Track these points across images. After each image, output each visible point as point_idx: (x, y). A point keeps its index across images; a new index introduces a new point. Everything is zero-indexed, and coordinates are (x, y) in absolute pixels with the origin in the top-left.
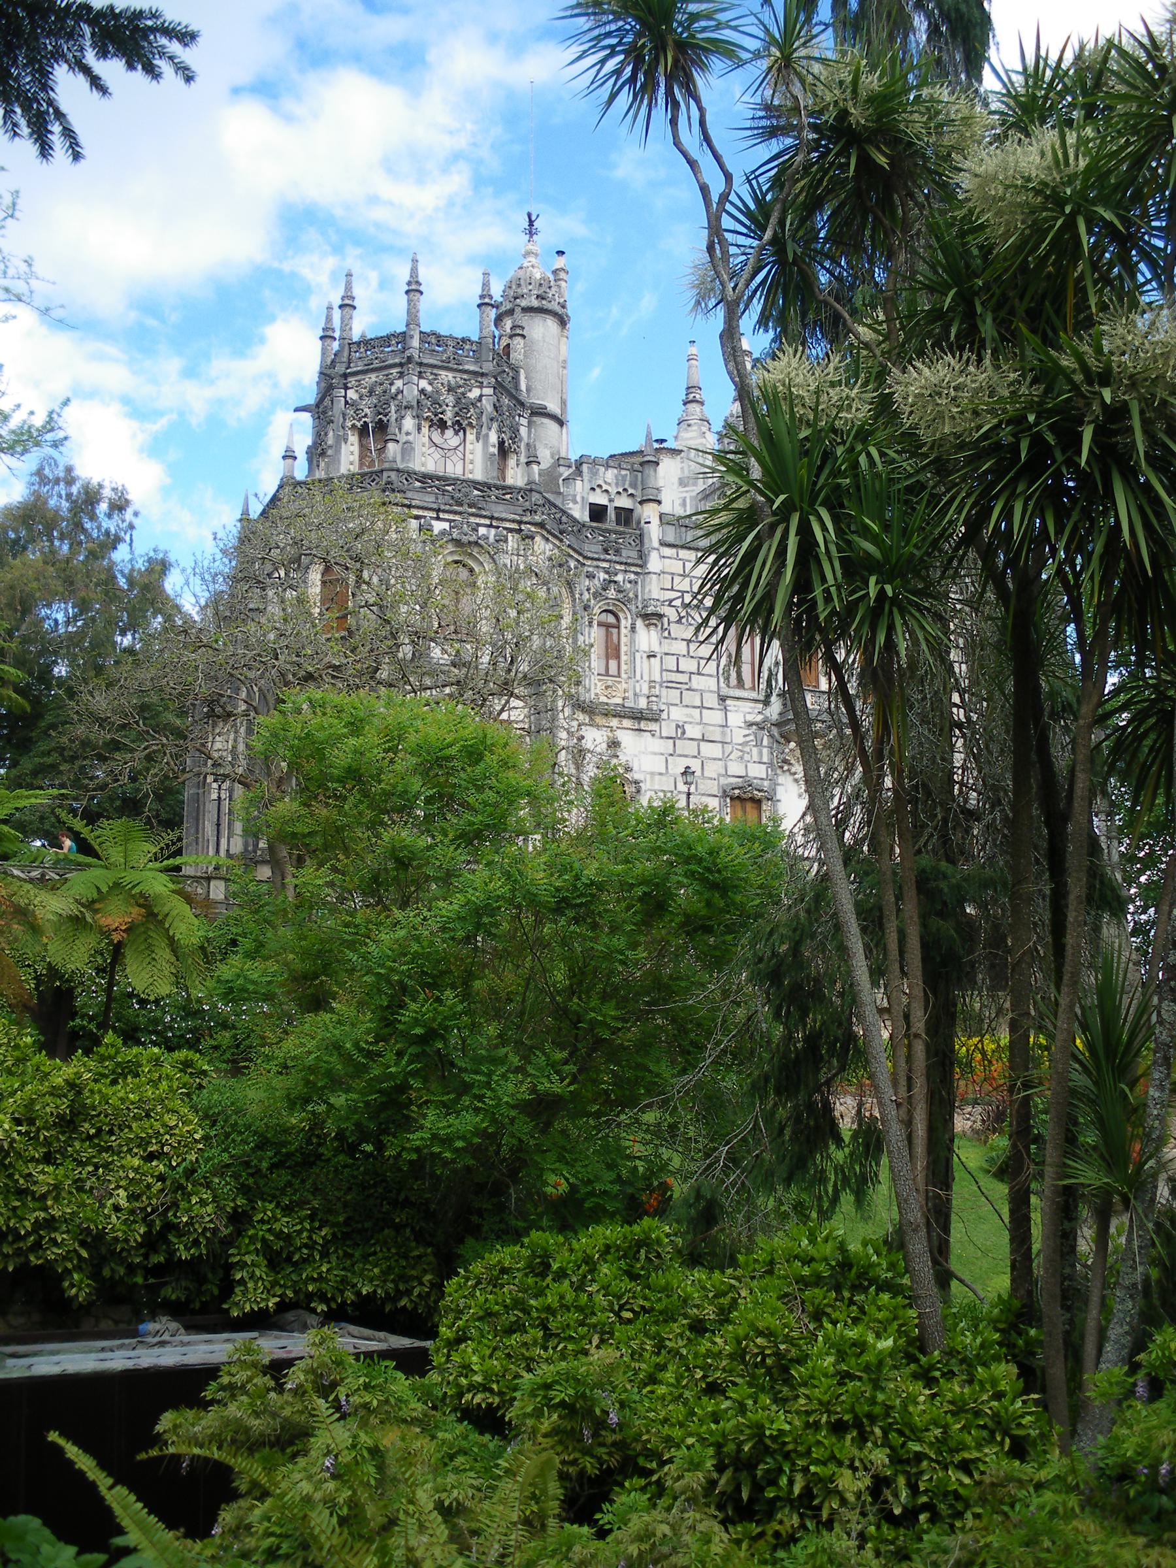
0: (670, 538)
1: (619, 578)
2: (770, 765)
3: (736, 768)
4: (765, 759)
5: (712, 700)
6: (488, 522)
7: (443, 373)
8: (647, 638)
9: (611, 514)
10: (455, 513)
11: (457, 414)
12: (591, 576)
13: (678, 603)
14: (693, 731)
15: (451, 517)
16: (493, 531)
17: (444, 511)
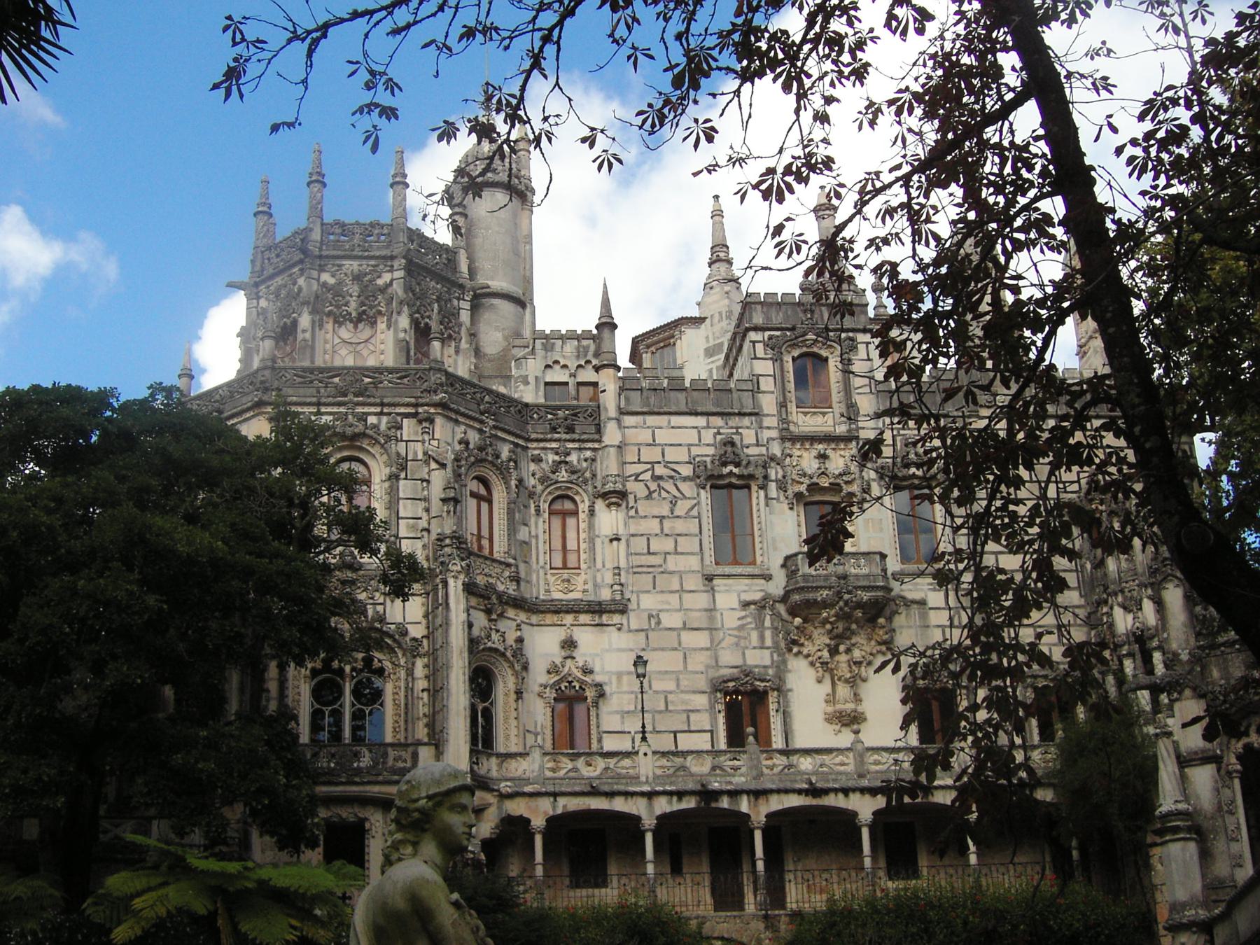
1: (573, 458)
2: (776, 646)
3: (729, 658)
4: (769, 642)
5: (694, 582)
6: (378, 410)
8: (609, 520)
9: (572, 388)
10: (340, 404)
11: (362, 304)
12: (537, 460)
13: (647, 476)
14: (669, 620)
15: (335, 409)
16: (385, 419)
17: (326, 405)
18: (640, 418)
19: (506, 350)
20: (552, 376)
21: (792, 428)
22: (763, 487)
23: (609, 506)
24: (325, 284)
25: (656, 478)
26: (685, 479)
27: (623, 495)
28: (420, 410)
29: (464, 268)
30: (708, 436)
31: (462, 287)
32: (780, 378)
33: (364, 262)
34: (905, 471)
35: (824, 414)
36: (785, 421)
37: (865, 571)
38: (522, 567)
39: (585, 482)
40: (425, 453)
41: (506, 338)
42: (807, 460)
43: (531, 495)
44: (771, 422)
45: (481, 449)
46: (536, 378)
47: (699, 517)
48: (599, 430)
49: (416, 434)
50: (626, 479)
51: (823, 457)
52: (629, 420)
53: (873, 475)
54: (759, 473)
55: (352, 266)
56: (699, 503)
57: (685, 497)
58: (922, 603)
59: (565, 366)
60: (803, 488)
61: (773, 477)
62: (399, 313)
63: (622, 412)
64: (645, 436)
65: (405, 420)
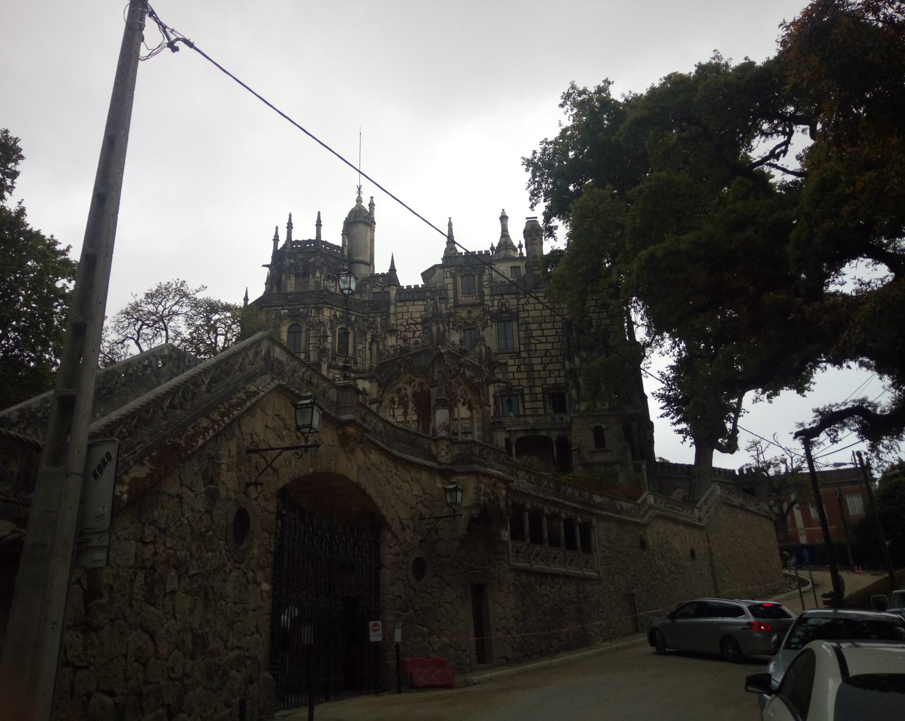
0: (402, 298)
12: (366, 320)
23: (391, 335)
24: (291, 264)
25: (408, 324)
26: (419, 324)
27: (396, 331)
29: (346, 253)
32: (455, 284)
38: (359, 360)
42: (463, 314)
43: (365, 333)
44: (452, 300)
45: (341, 317)
48: (389, 308)
50: (397, 325)
51: (470, 312)
52: (399, 304)
55: (301, 256)
58: (506, 364)
63: (397, 301)
64: (405, 309)
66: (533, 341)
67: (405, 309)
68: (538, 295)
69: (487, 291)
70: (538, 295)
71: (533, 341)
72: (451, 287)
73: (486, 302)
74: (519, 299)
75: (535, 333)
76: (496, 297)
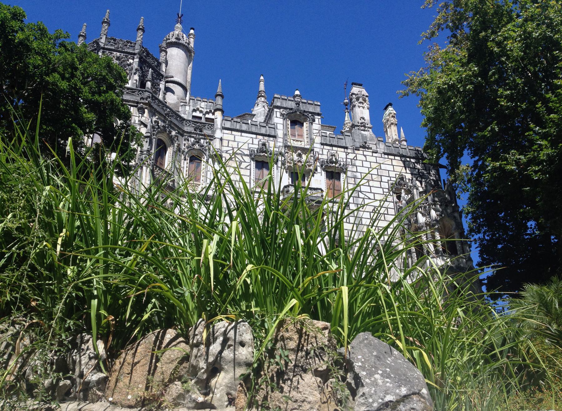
7: (115, 53)
13: (231, 152)
18: (229, 132)
19: (178, 103)
20: (194, 114)
21: (289, 144)
22: (276, 163)
26: (247, 155)
28: (139, 105)
30: (256, 141)
31: (162, 76)
32: (285, 127)
33: (122, 54)
34: (331, 165)
35: (301, 141)
36: (285, 140)
37: (316, 195)
39: (206, 150)
40: (139, 121)
41: (178, 99)
44: (281, 140)
46: (189, 113)
47: (250, 169)
48: (214, 132)
49: (136, 113)
51: (300, 155)
53: (318, 164)
54: (275, 157)
56: (250, 165)
57: (245, 162)
59: (201, 112)
60: (292, 165)
61: (280, 159)
62: (135, 74)
64: (231, 137)
65: (132, 108)
66: (361, 195)
67: (231, 137)
68: (365, 153)
69: (318, 140)
70: (365, 153)
71: (361, 195)
72: (280, 127)
73: (315, 150)
74: (347, 154)
75: (363, 188)
76: (325, 147)
